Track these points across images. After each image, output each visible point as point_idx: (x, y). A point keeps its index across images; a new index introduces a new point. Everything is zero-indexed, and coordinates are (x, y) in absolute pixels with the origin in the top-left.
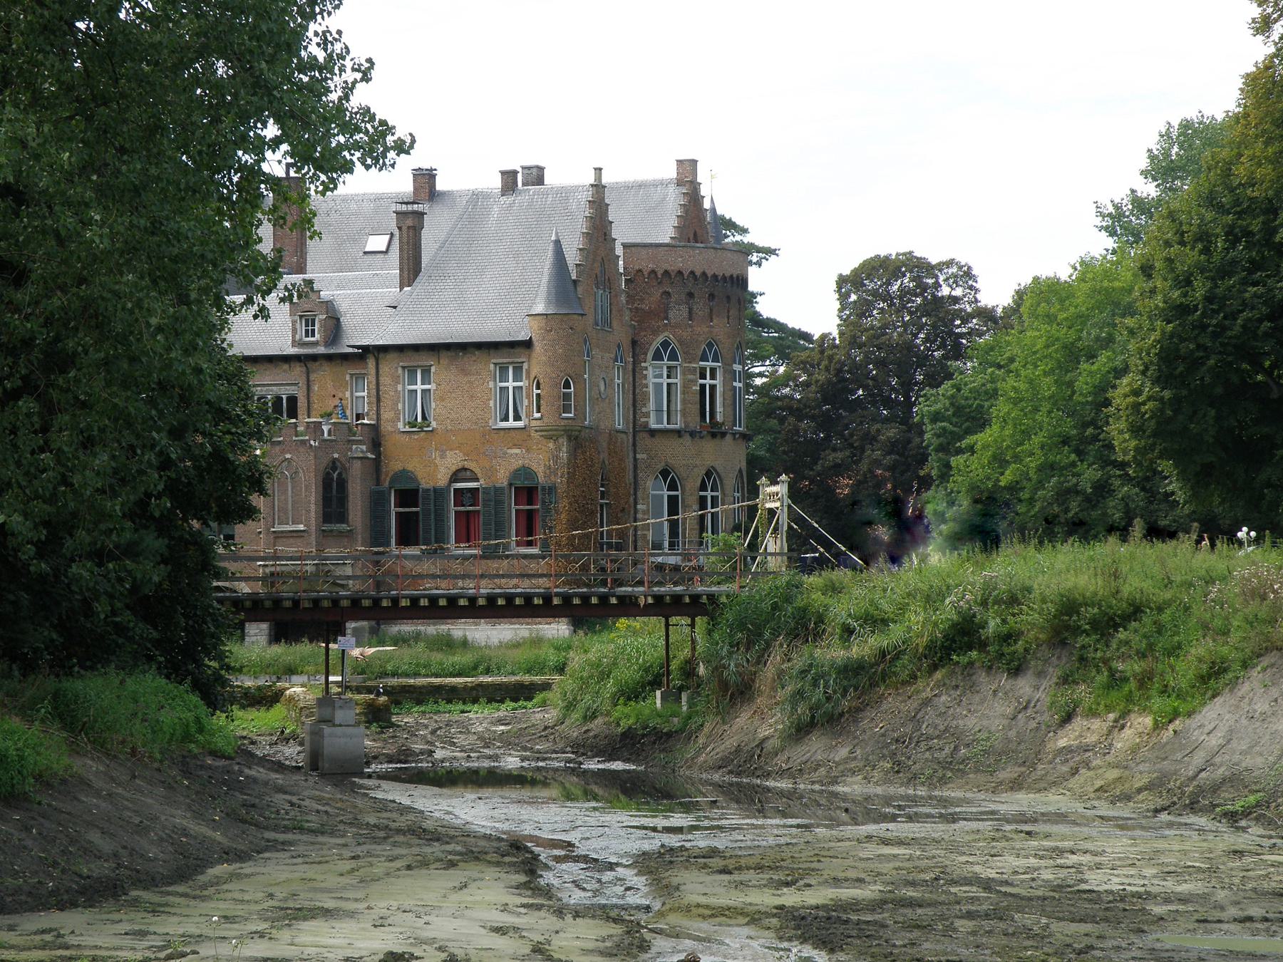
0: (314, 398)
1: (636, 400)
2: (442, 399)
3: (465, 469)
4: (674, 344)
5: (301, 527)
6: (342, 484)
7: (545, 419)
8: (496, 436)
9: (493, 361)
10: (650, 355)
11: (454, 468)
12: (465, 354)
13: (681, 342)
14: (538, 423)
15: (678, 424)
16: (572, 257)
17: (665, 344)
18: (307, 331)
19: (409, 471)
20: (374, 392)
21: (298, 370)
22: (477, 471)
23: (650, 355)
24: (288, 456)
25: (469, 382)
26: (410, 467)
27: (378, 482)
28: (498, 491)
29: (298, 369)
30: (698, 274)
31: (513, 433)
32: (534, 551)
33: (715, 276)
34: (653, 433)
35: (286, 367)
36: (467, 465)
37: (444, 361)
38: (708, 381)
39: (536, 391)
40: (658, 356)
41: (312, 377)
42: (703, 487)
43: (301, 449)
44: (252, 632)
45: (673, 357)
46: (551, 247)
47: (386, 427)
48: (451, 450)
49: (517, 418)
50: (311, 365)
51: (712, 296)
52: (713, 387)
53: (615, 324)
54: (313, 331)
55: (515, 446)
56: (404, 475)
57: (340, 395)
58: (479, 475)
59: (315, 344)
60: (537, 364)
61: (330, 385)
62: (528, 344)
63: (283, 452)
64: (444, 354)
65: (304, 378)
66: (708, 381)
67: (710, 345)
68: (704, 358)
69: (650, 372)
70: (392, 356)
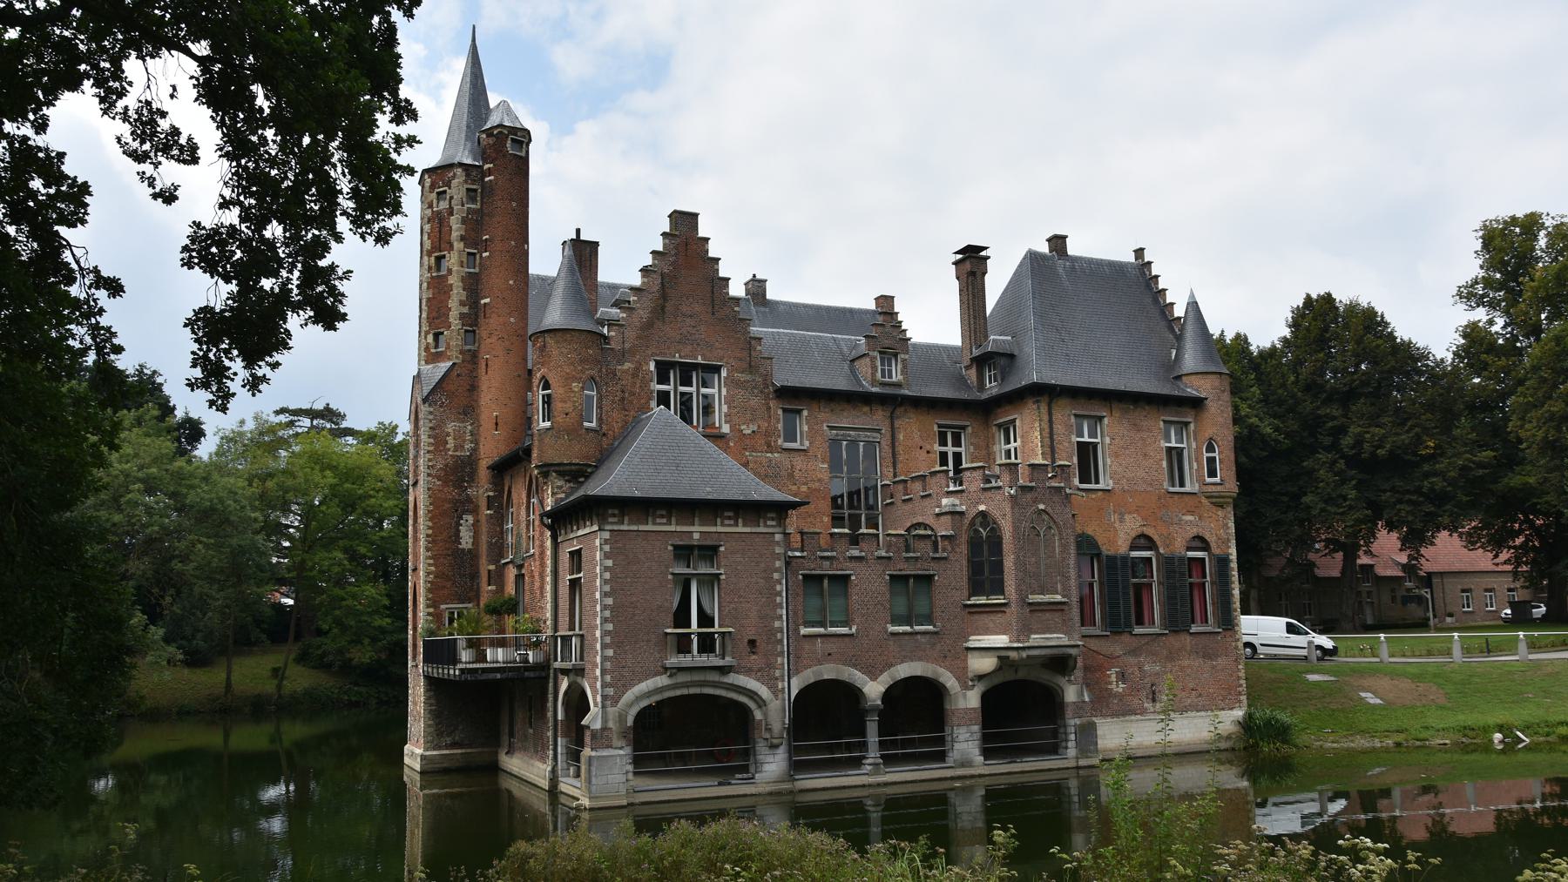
0: (900, 449)
2: (1116, 455)
3: (1143, 536)
5: (1058, 598)
7: (1227, 486)
8: (1171, 500)
9: (1162, 418)
11: (1134, 534)
12: (1136, 408)
14: (1219, 488)
18: (883, 371)
19: (1088, 536)
20: (1047, 440)
21: (879, 418)
22: (1156, 538)
24: (1042, 507)
25: (1143, 439)
26: (1090, 532)
29: (880, 413)
31: (1185, 496)
35: (866, 409)
37: (1117, 414)
39: (1206, 455)
41: (897, 423)
43: (1056, 499)
44: (961, 738)
48: (1129, 513)
50: (899, 411)
54: (890, 371)
55: (1191, 513)
57: (928, 447)
58: (1158, 543)
59: (898, 385)
61: (916, 435)
63: (1036, 501)
65: (887, 422)
70: (1063, 402)
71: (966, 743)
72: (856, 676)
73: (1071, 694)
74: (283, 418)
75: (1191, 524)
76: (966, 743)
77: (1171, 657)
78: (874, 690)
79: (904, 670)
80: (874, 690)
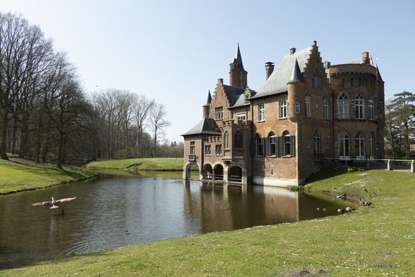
1: (334, 111)
4: (346, 94)
6: (241, 136)
10: (338, 98)
13: (349, 93)
15: (348, 117)
16: (302, 67)
17: (343, 94)
23: (338, 98)
27: (253, 136)
28: (279, 138)
30: (354, 72)
32: (289, 156)
33: (361, 74)
34: (339, 121)
36: (273, 131)
38: (359, 105)
40: (341, 98)
42: (357, 137)
45: (346, 98)
46: (295, 63)
47: (254, 122)
49: (285, 116)
51: (360, 79)
52: (361, 107)
53: (323, 88)
56: (258, 135)
60: (290, 99)
62: (283, 94)
64: (267, 99)
66: (359, 105)
67: (359, 94)
68: (357, 98)
69: (338, 103)
71: (225, 177)
72: (211, 163)
73: (243, 170)
74: (398, 97)
75: (283, 128)
76: (225, 177)
77: (277, 163)
78: (213, 166)
79: (217, 163)
80: (213, 166)
